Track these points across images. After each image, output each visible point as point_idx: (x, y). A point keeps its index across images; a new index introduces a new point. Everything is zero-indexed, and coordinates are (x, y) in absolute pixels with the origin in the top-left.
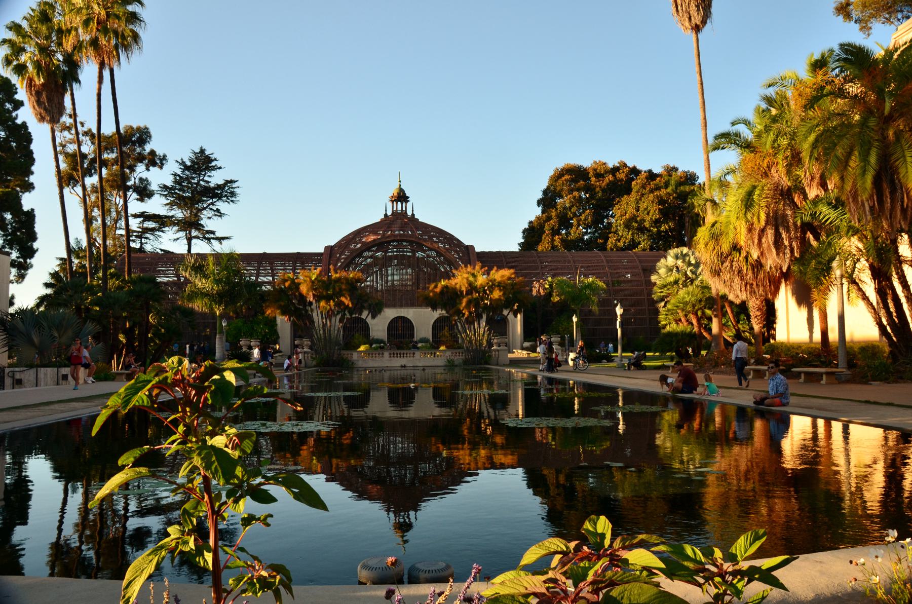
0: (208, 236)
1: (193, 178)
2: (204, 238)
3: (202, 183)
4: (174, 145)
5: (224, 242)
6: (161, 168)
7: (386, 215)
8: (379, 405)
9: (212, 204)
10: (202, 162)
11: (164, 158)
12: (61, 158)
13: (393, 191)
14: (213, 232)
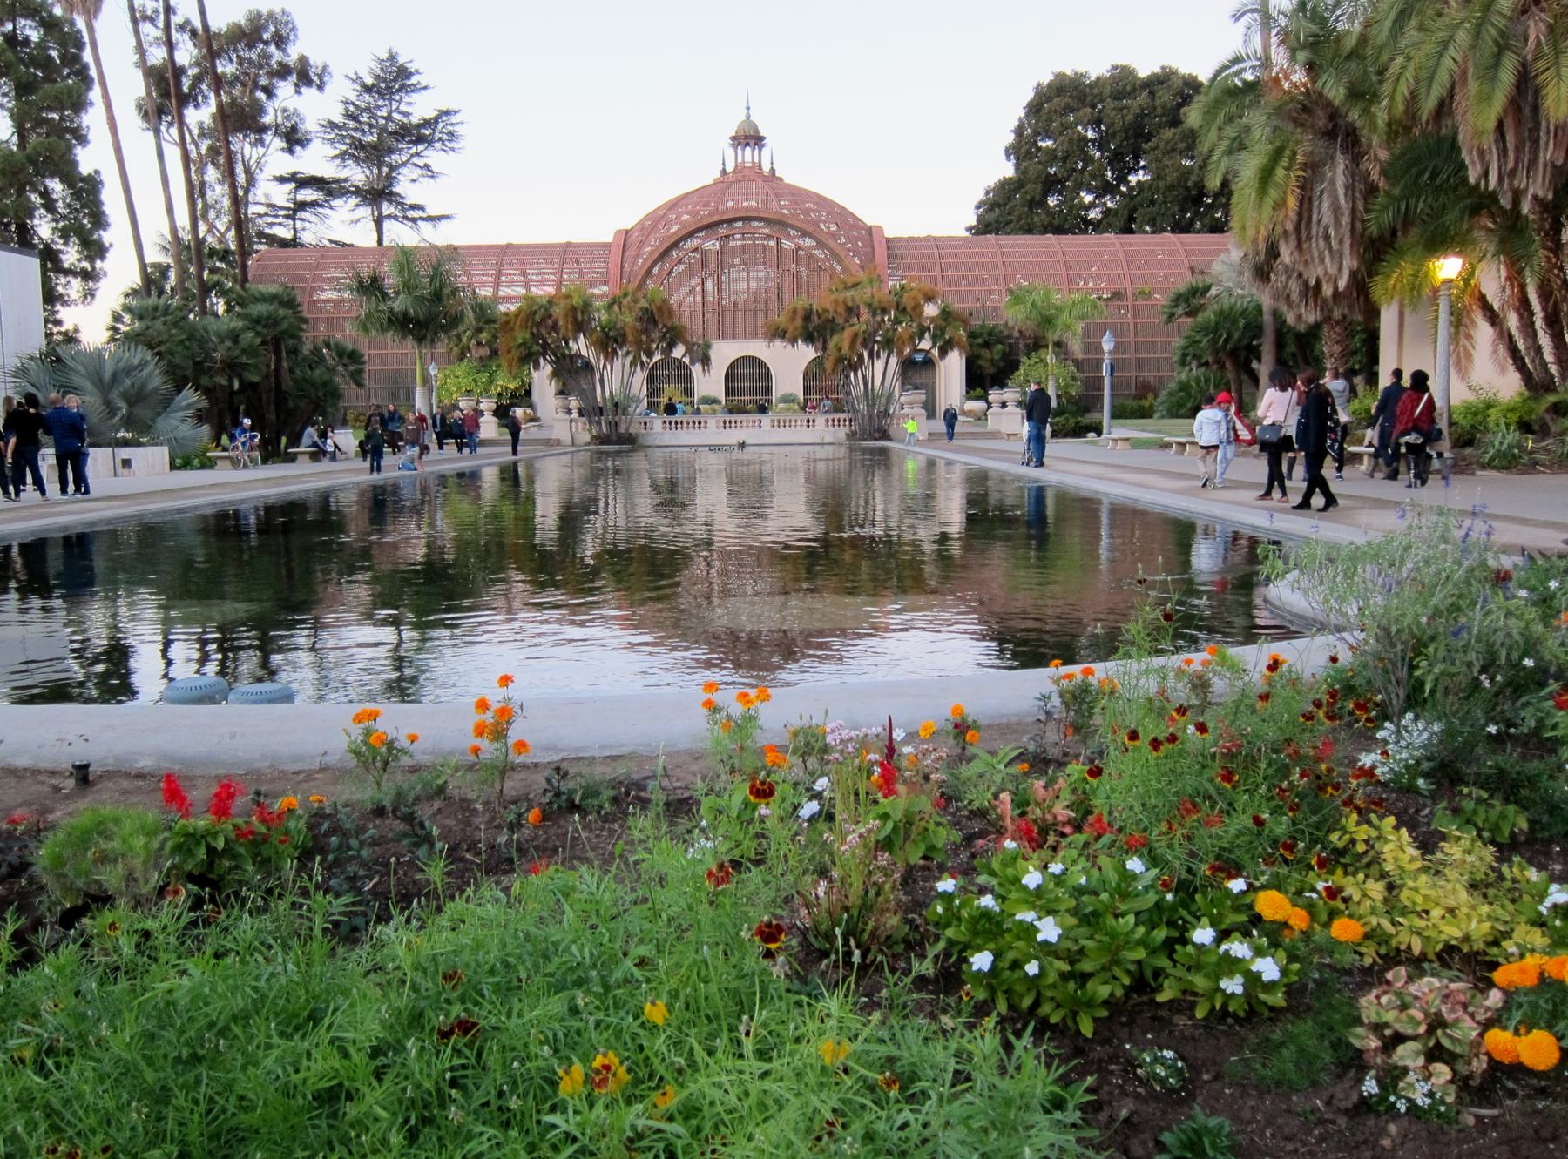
0: (412, 214)
1: (379, 108)
2: (405, 217)
5: (443, 224)
6: (320, 87)
7: (724, 172)
9: (417, 154)
10: (394, 79)
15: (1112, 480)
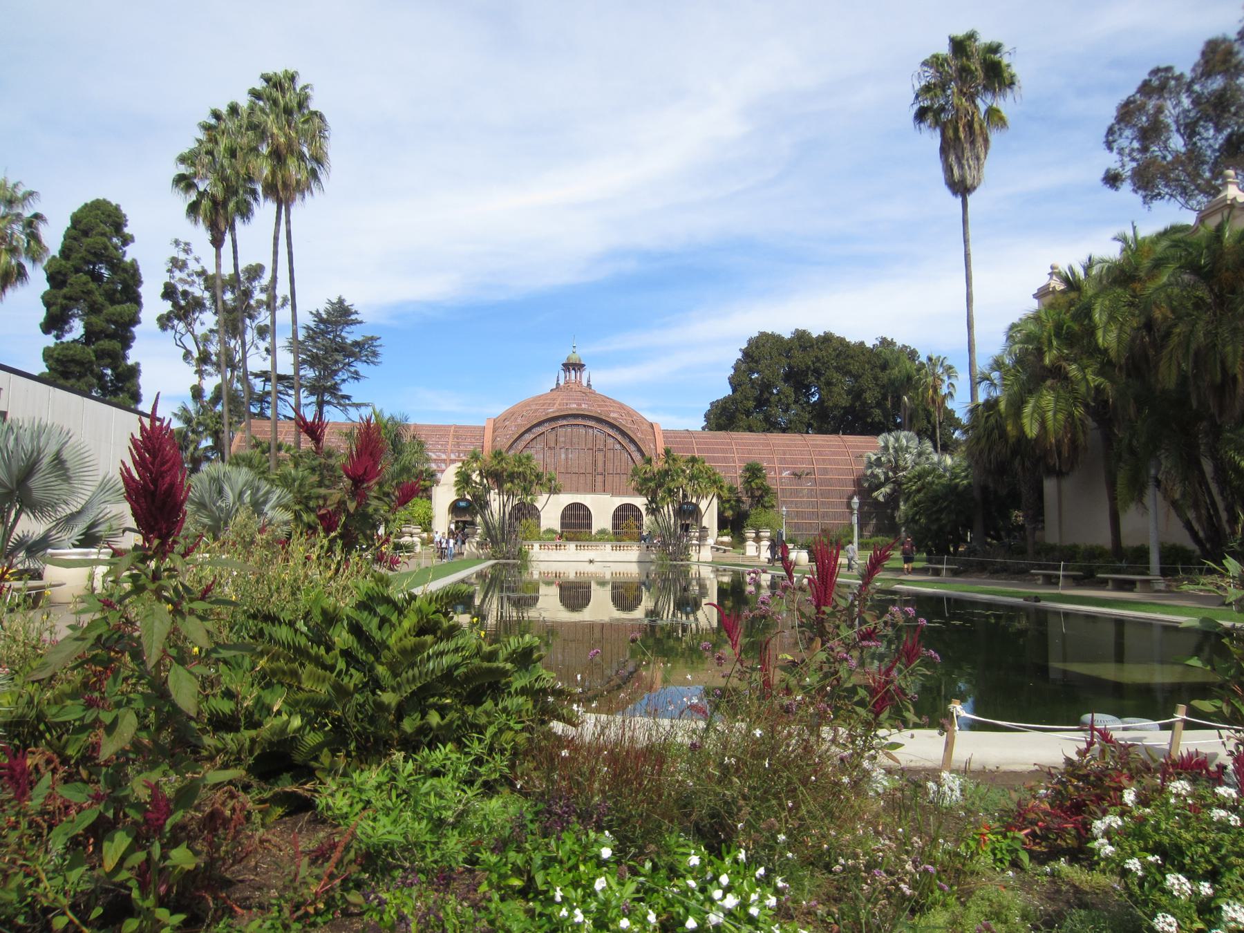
1: (329, 333)
3: (338, 339)
7: (558, 384)
8: (549, 607)
9: (349, 364)
10: (341, 314)
14: (348, 398)
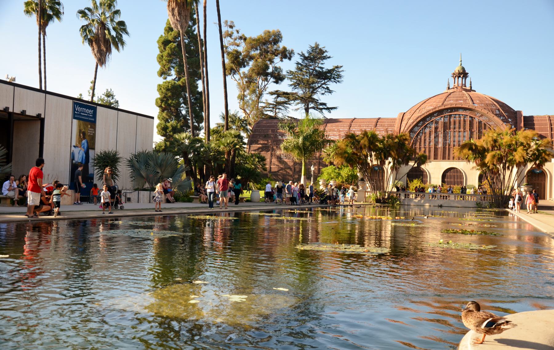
0: (321, 107)
1: (311, 66)
3: (317, 69)
4: (298, 43)
5: (332, 111)
6: (290, 59)
9: (324, 84)
10: (317, 54)
11: (292, 53)
12: (225, 55)
13: (457, 69)
15: (420, 302)
